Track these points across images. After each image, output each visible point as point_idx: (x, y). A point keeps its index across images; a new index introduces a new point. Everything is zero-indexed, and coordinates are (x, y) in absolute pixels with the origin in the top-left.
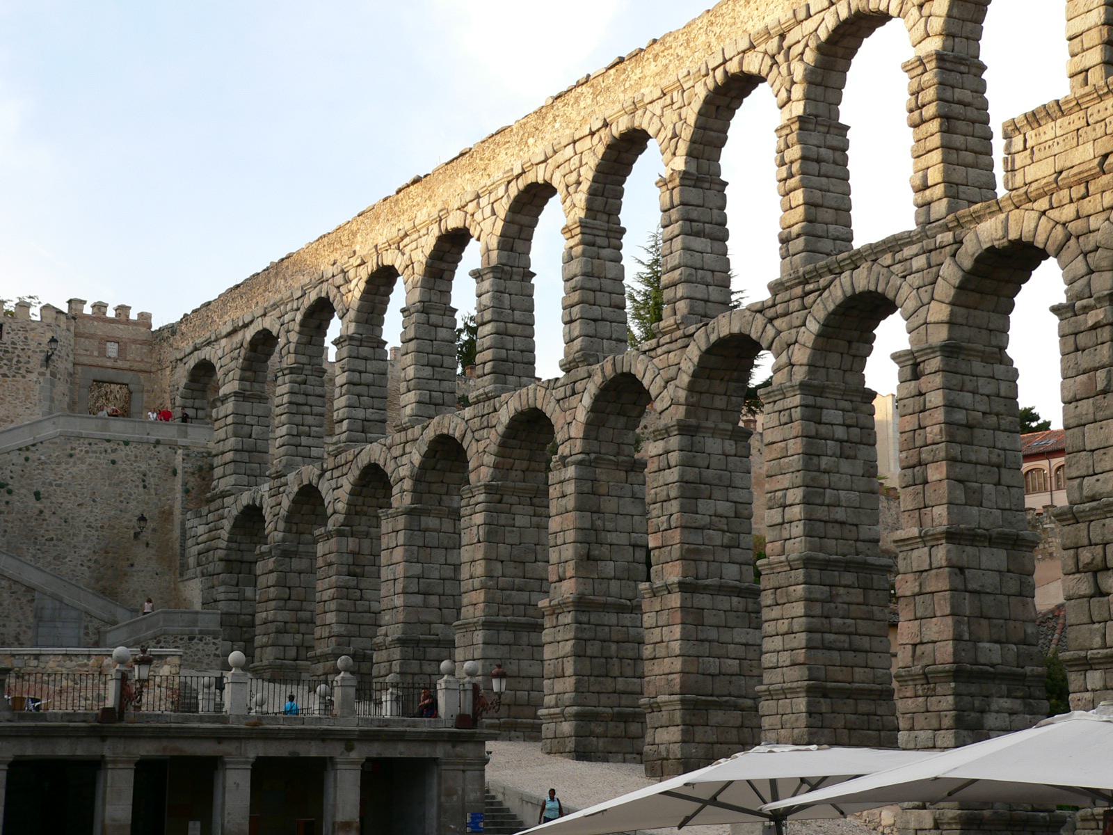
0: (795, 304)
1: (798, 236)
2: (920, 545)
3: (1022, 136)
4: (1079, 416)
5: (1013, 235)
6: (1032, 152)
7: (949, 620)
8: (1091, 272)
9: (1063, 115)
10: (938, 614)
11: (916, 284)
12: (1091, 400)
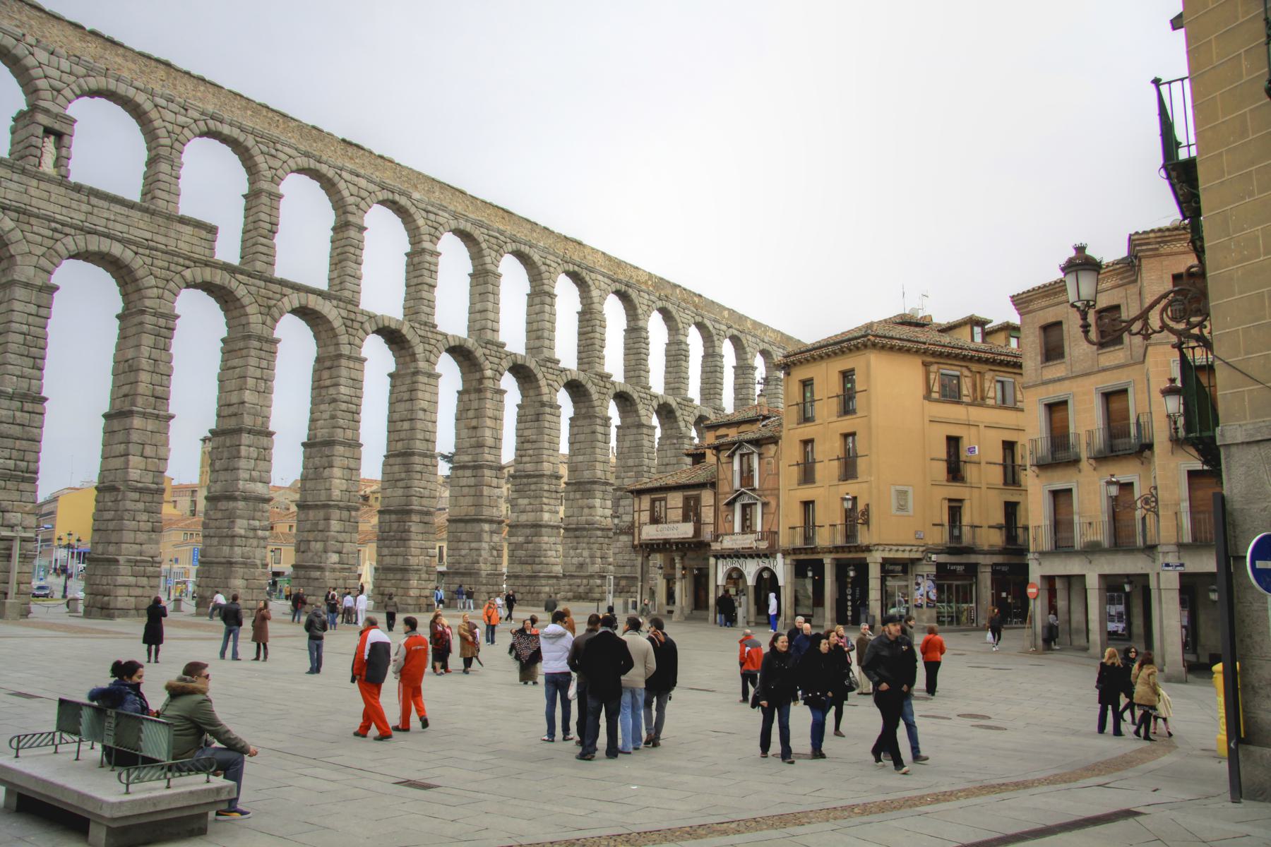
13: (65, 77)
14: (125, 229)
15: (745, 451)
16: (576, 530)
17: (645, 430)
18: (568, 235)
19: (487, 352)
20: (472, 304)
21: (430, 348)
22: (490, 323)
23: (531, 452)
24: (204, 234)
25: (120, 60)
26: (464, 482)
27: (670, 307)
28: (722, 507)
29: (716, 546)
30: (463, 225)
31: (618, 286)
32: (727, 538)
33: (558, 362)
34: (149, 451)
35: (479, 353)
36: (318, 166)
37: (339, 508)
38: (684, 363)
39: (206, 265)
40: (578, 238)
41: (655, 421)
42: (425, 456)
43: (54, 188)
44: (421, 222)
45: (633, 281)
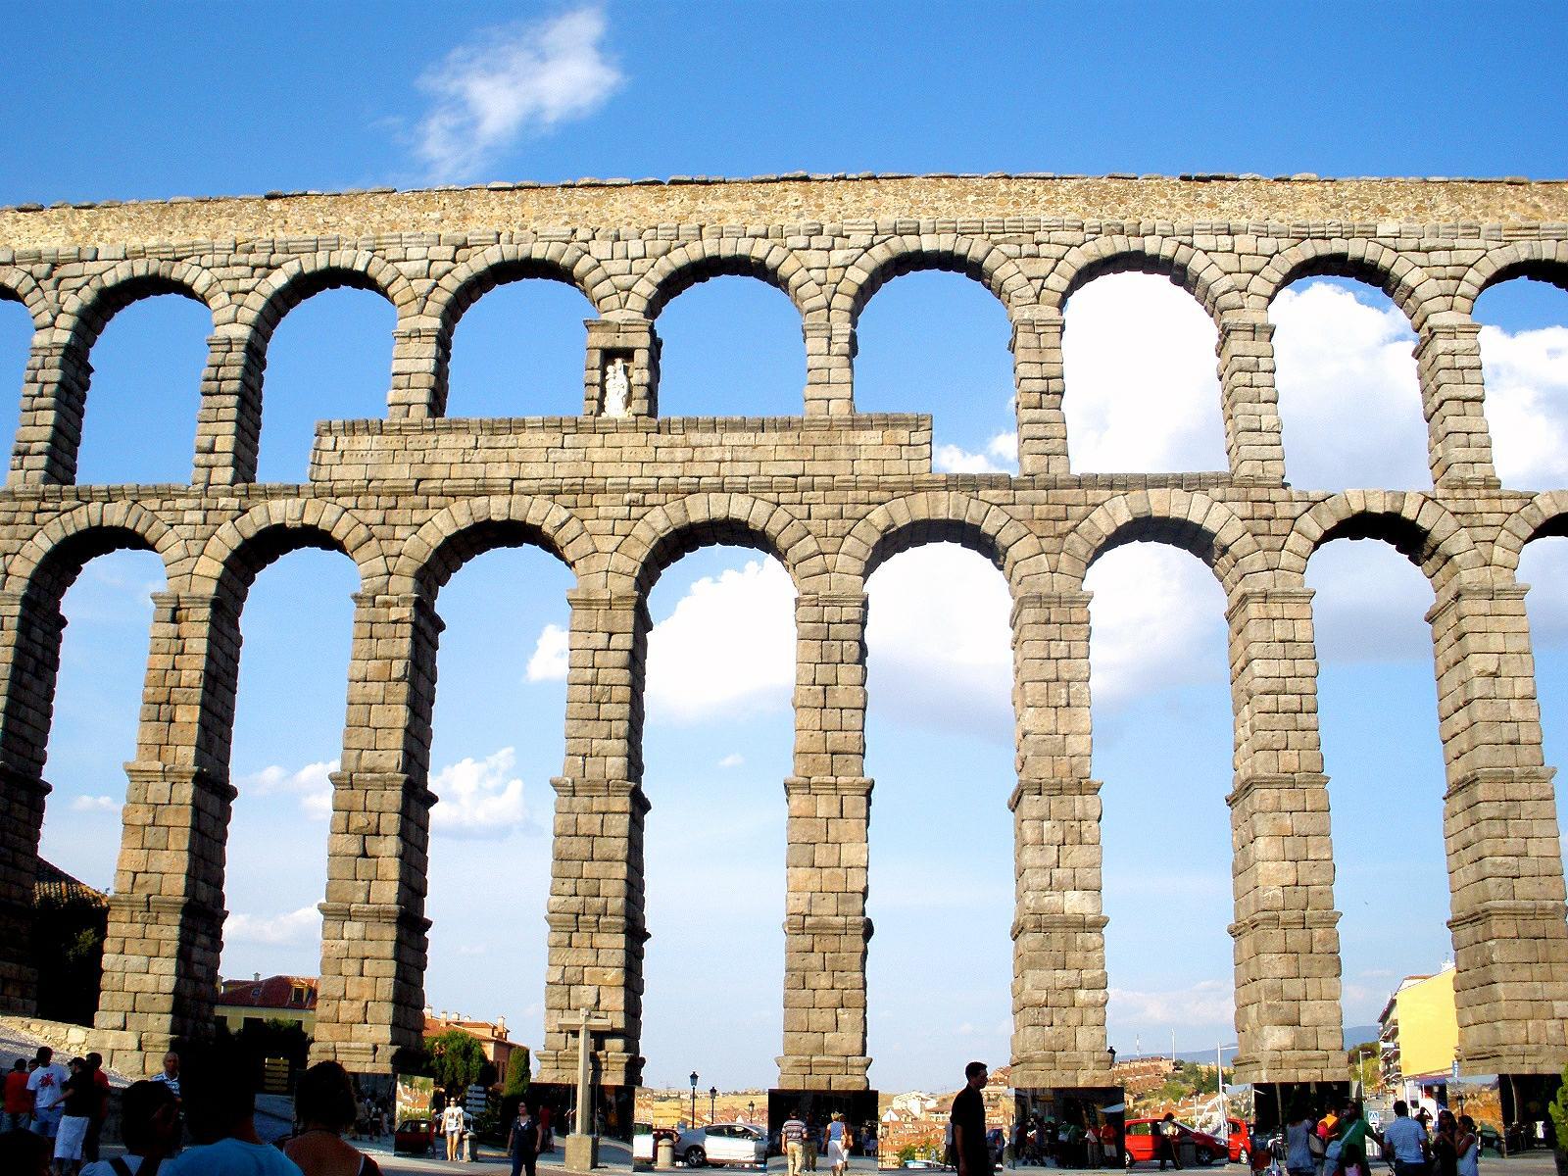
0: (27, 517)
1: (40, 453)
2: (159, 779)
3: (333, 438)
4: (369, 695)
5: (309, 520)
6: (342, 455)
7: (185, 856)
8: (390, 574)
9: (381, 434)
10: (172, 846)
11: (187, 535)
12: (382, 684)
13: (637, 266)
14: (752, 469)
21: (1490, 534)
24: (903, 435)
25: (722, 205)
30: (1522, 251)
34: (822, 855)
36: (1135, 244)
37: (1287, 925)
39: (916, 490)
43: (629, 439)
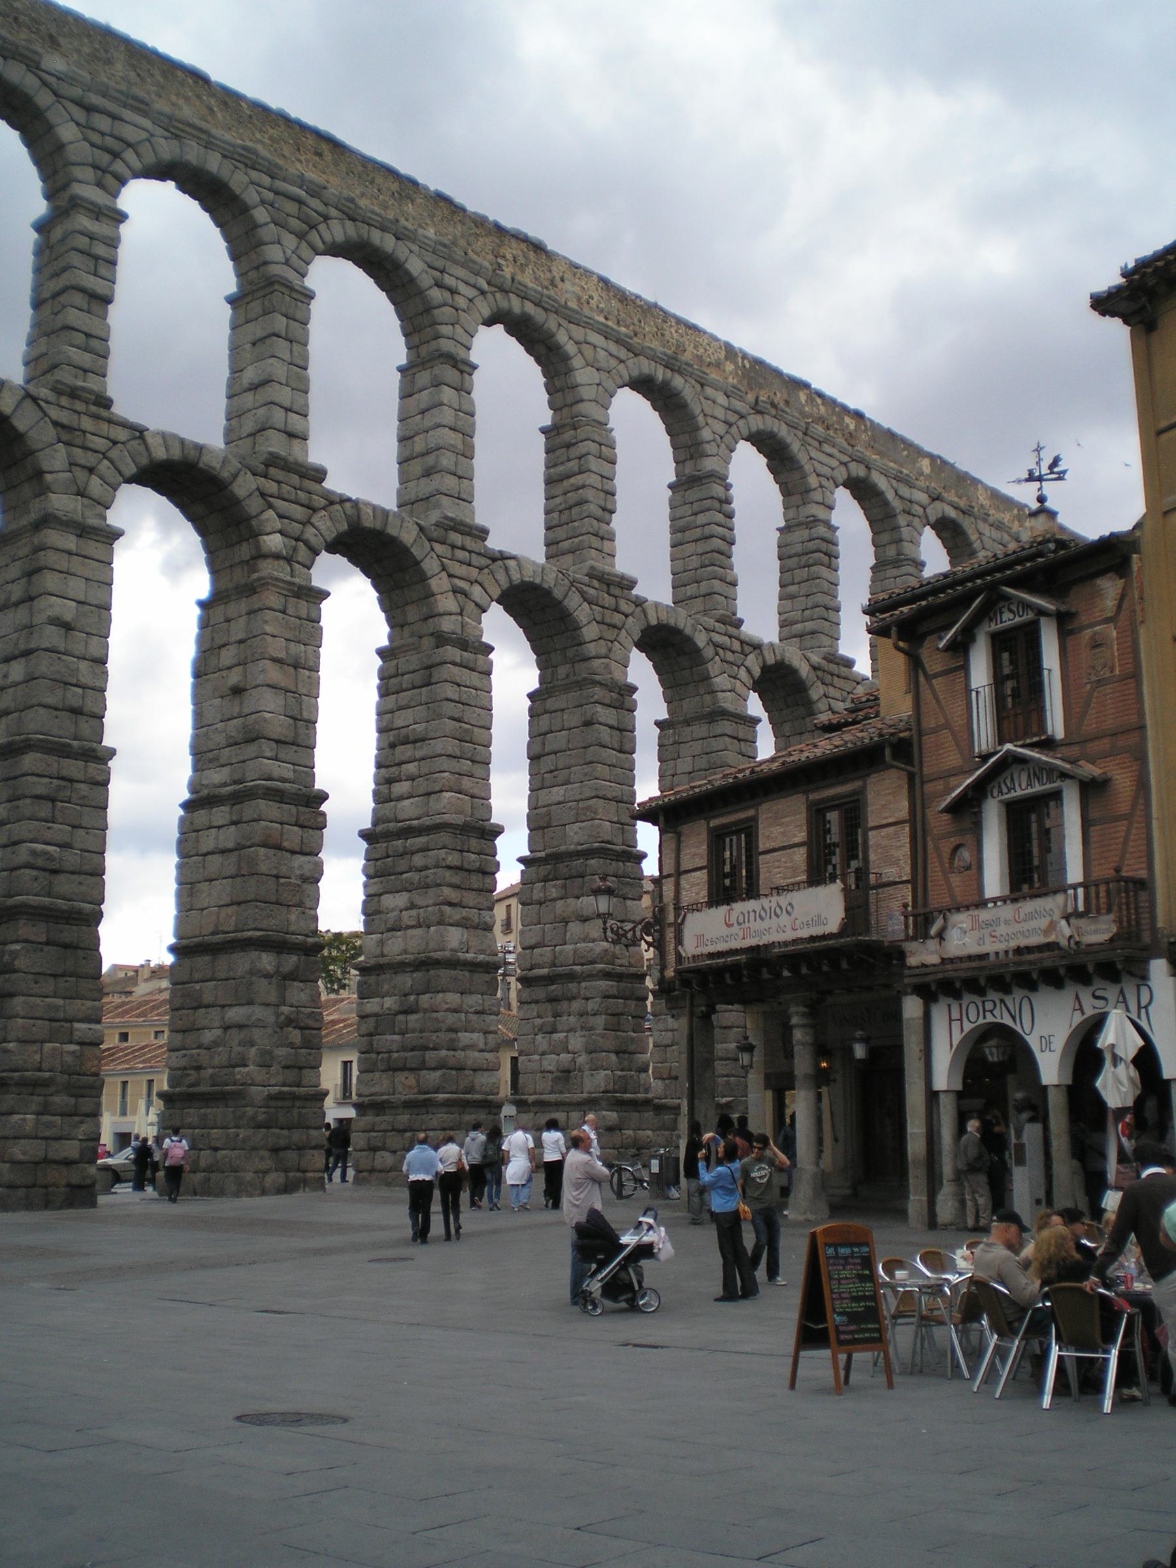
15: (1008, 619)
16: (550, 979)
17: (726, 727)
18: (507, 223)
19: (272, 487)
20: (236, 371)
22: (278, 415)
23: (411, 768)
26: (209, 841)
27: (783, 431)
28: (938, 821)
29: (923, 955)
30: (193, 153)
31: (646, 367)
32: (961, 920)
33: (483, 533)
35: (245, 485)
38: (824, 572)
40: (533, 232)
41: (755, 706)
42: (63, 751)
44: (67, 132)
45: (687, 357)
